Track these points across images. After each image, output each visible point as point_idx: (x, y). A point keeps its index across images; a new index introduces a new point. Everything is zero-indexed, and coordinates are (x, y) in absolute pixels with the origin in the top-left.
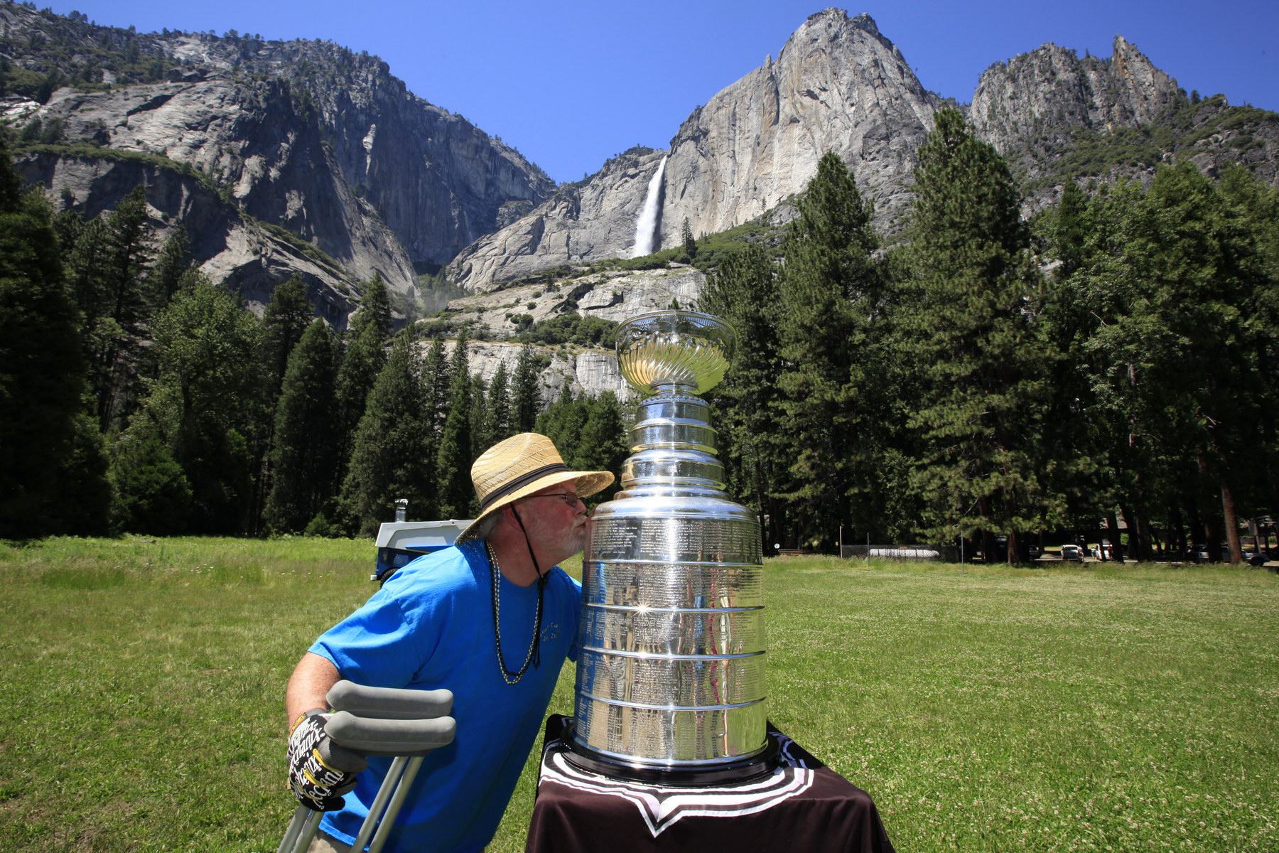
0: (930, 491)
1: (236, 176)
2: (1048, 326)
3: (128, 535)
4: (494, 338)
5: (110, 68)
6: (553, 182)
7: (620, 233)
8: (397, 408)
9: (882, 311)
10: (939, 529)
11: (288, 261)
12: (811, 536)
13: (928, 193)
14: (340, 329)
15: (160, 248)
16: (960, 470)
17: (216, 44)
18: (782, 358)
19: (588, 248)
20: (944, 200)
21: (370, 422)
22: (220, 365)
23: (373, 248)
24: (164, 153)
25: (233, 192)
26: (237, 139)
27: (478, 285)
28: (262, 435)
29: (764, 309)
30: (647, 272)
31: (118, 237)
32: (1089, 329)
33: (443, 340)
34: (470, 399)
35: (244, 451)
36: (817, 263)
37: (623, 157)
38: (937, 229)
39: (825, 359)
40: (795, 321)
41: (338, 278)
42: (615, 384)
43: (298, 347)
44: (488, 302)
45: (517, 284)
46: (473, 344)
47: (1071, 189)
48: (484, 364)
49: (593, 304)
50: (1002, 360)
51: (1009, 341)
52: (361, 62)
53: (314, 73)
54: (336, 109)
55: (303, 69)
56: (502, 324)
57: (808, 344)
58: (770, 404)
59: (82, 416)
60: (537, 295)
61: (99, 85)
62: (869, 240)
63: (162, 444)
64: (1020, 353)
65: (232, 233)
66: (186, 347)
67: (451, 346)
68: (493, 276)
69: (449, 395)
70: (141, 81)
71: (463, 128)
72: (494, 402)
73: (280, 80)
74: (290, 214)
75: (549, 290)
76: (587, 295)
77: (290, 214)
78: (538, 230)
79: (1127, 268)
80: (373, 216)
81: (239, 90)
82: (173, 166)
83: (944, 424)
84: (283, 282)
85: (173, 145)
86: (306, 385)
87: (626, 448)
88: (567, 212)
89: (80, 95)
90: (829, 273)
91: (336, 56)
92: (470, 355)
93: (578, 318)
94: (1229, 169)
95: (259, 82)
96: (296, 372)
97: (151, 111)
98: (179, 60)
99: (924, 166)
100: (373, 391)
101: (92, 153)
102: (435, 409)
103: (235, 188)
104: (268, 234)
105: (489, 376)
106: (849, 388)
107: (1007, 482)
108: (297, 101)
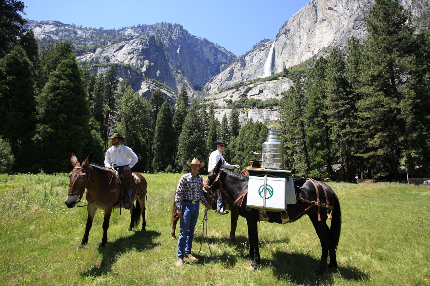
1: (142, 66)
5: (109, 41)
6: (236, 56)
7: (259, 70)
24: (123, 62)
26: (142, 55)
41: (172, 93)
48: (217, 116)
49: (252, 94)
52: (175, 27)
55: (159, 32)
56: (222, 103)
65: (142, 83)
68: (218, 89)
70: (117, 43)
71: (206, 43)
73: (152, 36)
74: (157, 75)
78: (232, 72)
81: (142, 40)
85: (126, 59)
88: (241, 65)
91: (167, 26)
93: (247, 99)
98: (126, 36)
104: (151, 82)
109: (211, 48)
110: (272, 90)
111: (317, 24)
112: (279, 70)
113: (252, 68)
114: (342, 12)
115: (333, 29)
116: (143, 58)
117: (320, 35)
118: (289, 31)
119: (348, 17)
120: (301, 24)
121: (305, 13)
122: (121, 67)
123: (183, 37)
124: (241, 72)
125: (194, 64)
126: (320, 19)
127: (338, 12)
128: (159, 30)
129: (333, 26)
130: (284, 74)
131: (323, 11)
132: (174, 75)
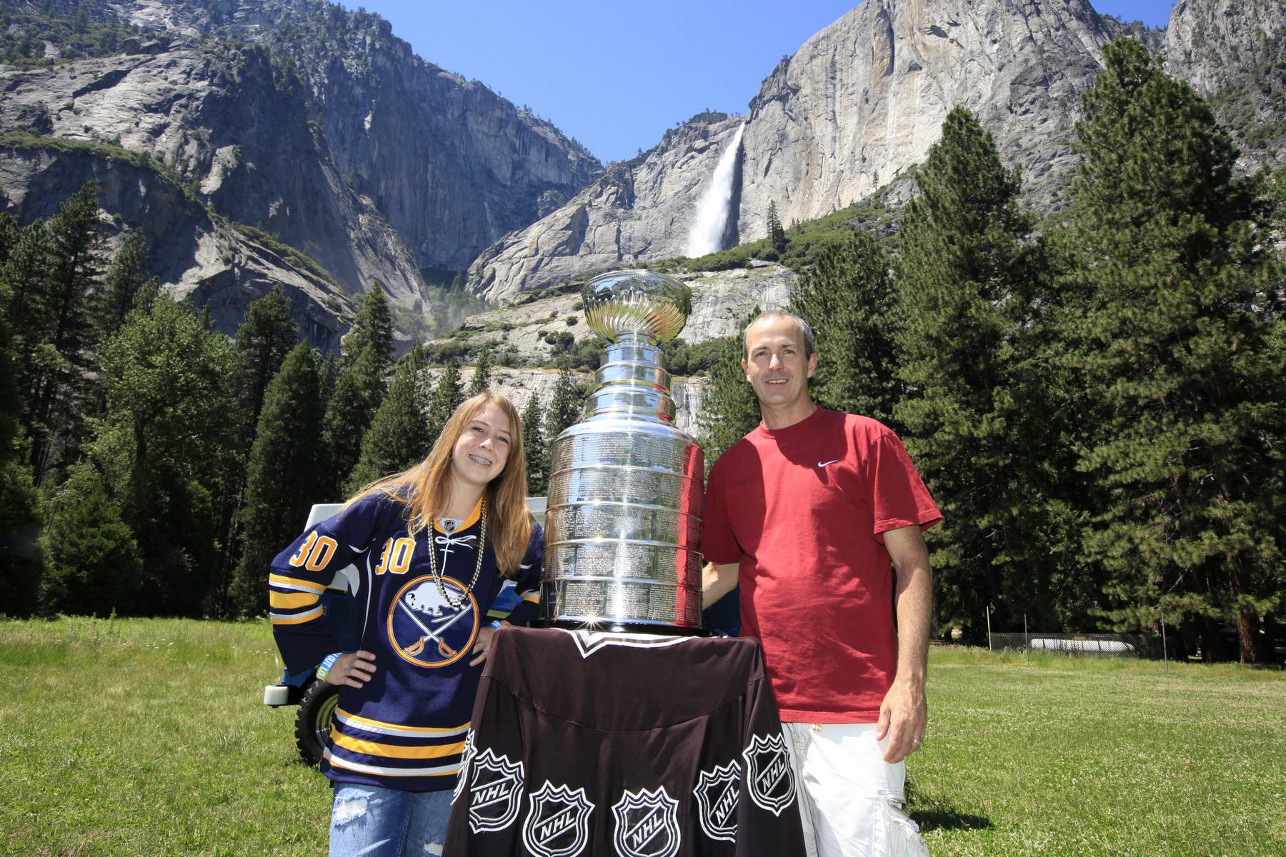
0: (1113, 558)
1: (204, 168)
3: (63, 617)
5: (54, 40)
6: (598, 162)
7: (684, 224)
8: (400, 453)
9: (1036, 314)
10: (1128, 611)
11: (266, 271)
12: (947, 621)
14: (330, 353)
15: (112, 257)
16: (1159, 530)
17: (181, 6)
18: (899, 381)
20: (1121, 160)
22: (182, 399)
23: (370, 252)
27: (503, 296)
28: (232, 491)
29: (875, 317)
31: (61, 245)
33: (458, 366)
35: (207, 509)
36: (944, 253)
39: (961, 381)
40: (916, 332)
41: (328, 292)
43: (278, 378)
44: (515, 317)
45: (553, 293)
46: (496, 371)
50: (1213, 374)
53: (300, 37)
54: (326, 81)
57: (935, 361)
59: (12, 465)
61: (40, 60)
62: (1015, 220)
63: (108, 500)
64: (1240, 364)
66: (138, 378)
68: (523, 282)
70: (91, 54)
71: (483, 98)
73: (258, 48)
74: (272, 212)
77: (272, 212)
78: (579, 224)
82: (128, 157)
83: (1132, 465)
84: (259, 297)
85: (129, 131)
86: (287, 425)
88: (616, 199)
89: (17, 73)
90: (961, 266)
91: (326, 16)
95: (233, 51)
96: (274, 409)
97: (103, 91)
98: (136, 27)
100: (370, 433)
101: (30, 143)
103: (203, 182)
104: (242, 237)
106: (993, 419)
107: (1228, 543)
108: (280, 76)
109: (501, 121)
110: (726, 305)
111: (893, 82)
112: (757, 232)
113: (656, 215)
114: (976, 47)
115: (945, 102)
116: (211, 135)
117: (903, 119)
118: (795, 91)
119: (993, 68)
120: (838, 74)
121: (852, 35)
122: (105, 162)
123: (388, 65)
125: (429, 176)
126: (904, 62)
127: (962, 47)
128: (289, 28)
129: (946, 92)
130: (771, 249)
131: (913, 35)
132: (344, 218)
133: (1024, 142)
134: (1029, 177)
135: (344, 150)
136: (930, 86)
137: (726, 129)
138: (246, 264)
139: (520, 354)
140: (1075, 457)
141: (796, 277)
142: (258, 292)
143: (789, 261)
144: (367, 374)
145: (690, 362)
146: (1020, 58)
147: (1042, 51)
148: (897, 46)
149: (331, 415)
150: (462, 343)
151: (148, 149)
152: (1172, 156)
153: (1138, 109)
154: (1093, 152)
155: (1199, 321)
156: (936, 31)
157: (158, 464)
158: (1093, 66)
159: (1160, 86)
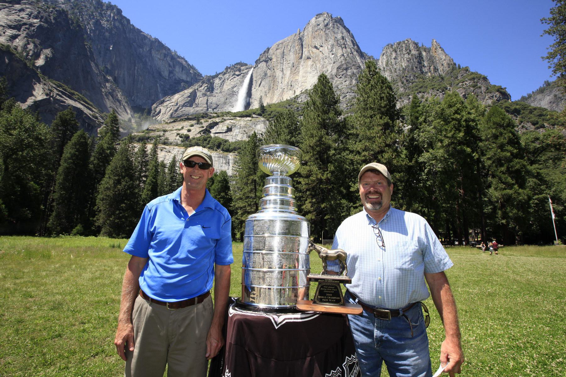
1: (37, 56)
2: (405, 152)
4: (171, 144)
6: (201, 75)
8: (122, 175)
9: (342, 141)
11: (65, 100)
13: (362, 95)
14: (93, 135)
19: (216, 106)
20: (368, 98)
21: (107, 182)
22: (26, 149)
23: (110, 97)
25: (34, 63)
28: (48, 186)
29: (293, 138)
30: (243, 119)
32: (420, 152)
33: (146, 144)
34: (158, 172)
36: (316, 120)
37: (234, 66)
38: (365, 109)
40: (306, 144)
41: (92, 111)
42: (227, 168)
43: (70, 143)
44: (168, 127)
45: (182, 120)
46: (160, 146)
47: (415, 98)
48: (165, 156)
51: (391, 157)
53: (82, 9)
54: (93, 28)
57: (311, 154)
58: (295, 179)
60: (192, 126)
64: (395, 162)
67: (149, 147)
68: (171, 115)
69: (148, 169)
71: (158, 45)
72: (170, 174)
73: (63, 10)
75: (198, 124)
76: (215, 127)
78: (193, 96)
79: (434, 131)
80: (111, 82)
87: (231, 196)
88: (207, 89)
92: (159, 151)
93: (211, 137)
94: (470, 95)
96: (69, 155)
99: (360, 83)
100: (110, 166)
102: (140, 175)
103: (36, 61)
104: (54, 86)
105: (168, 162)
106: (328, 173)
108: (73, 23)
109: (165, 54)
110: (244, 129)
112: (255, 105)
114: (327, 55)
118: (271, 60)
120: (285, 56)
121: (290, 44)
123: (120, 26)
124: (206, 98)
128: (77, 5)
132: (100, 83)
133: (339, 87)
134: (341, 98)
135: (100, 56)
136: (313, 65)
137: (247, 69)
138: (56, 96)
139: (170, 141)
140: (350, 186)
141: (267, 122)
142: (61, 108)
143: (266, 116)
144: (108, 144)
145: (230, 148)
146: (340, 61)
147: (346, 60)
148: (304, 50)
149: (93, 159)
150: (147, 135)
151: (10, 44)
152: (382, 98)
153: (373, 83)
154: (361, 94)
155: (385, 148)
156: (316, 47)
157: (14, 174)
158: (360, 67)
159: (379, 77)
